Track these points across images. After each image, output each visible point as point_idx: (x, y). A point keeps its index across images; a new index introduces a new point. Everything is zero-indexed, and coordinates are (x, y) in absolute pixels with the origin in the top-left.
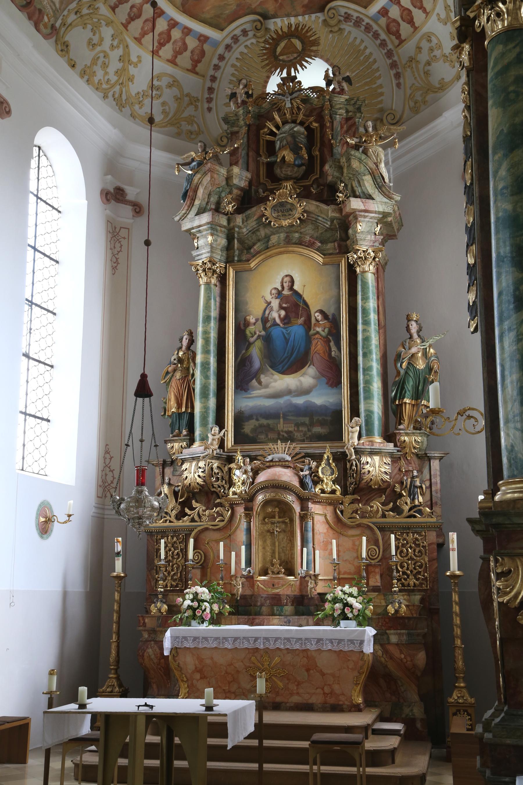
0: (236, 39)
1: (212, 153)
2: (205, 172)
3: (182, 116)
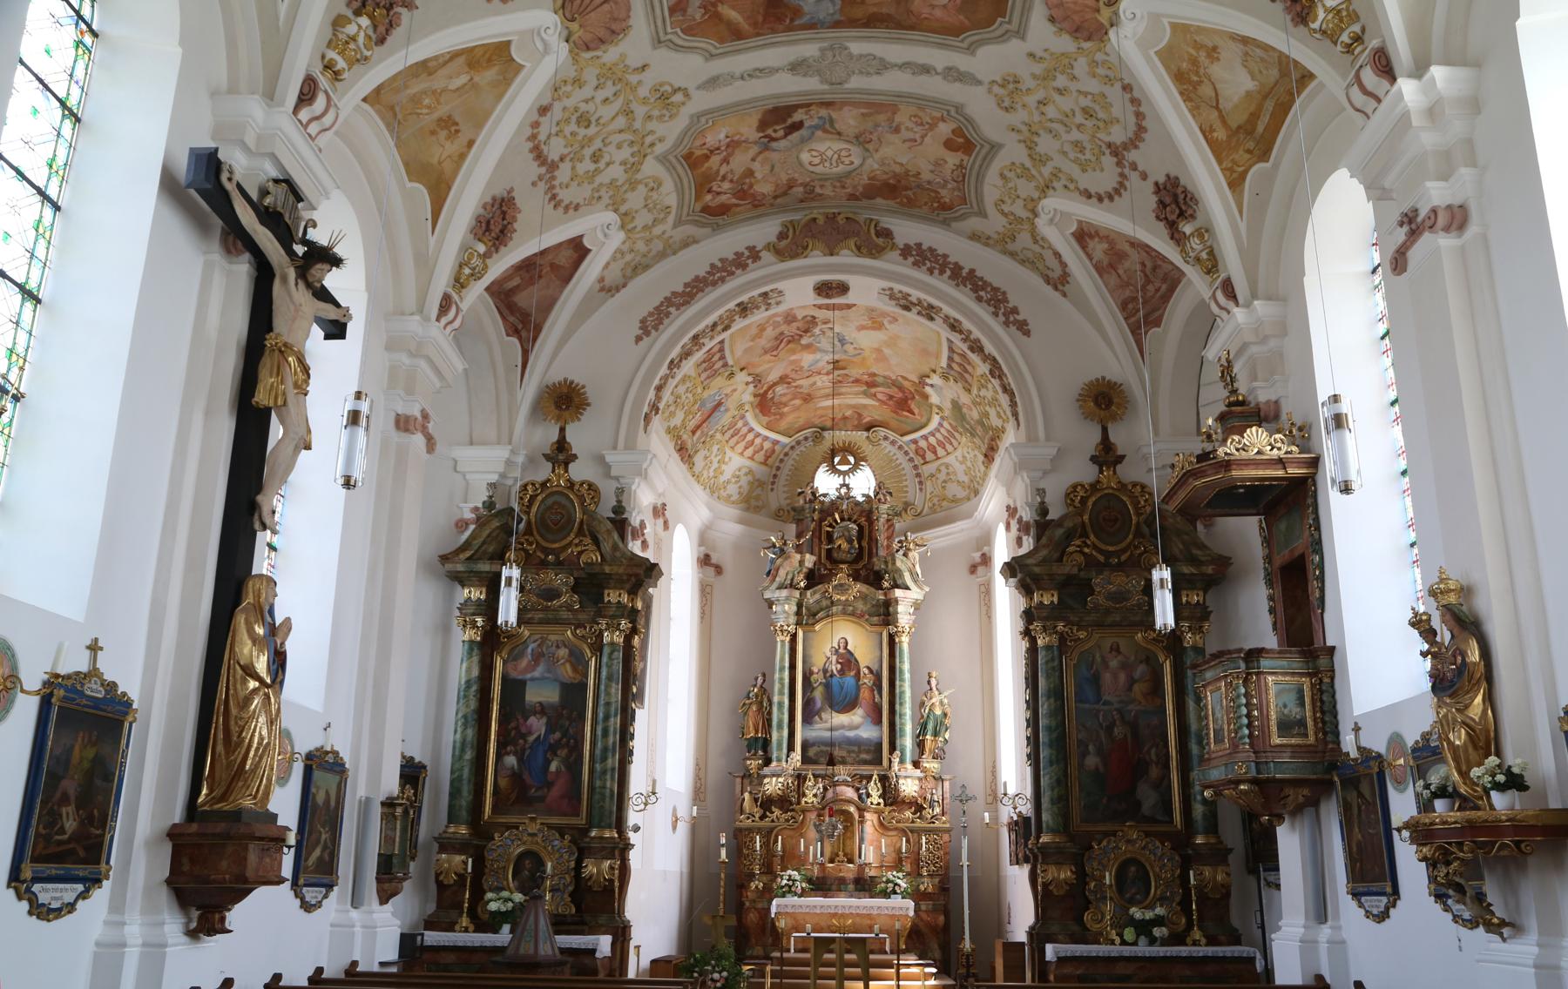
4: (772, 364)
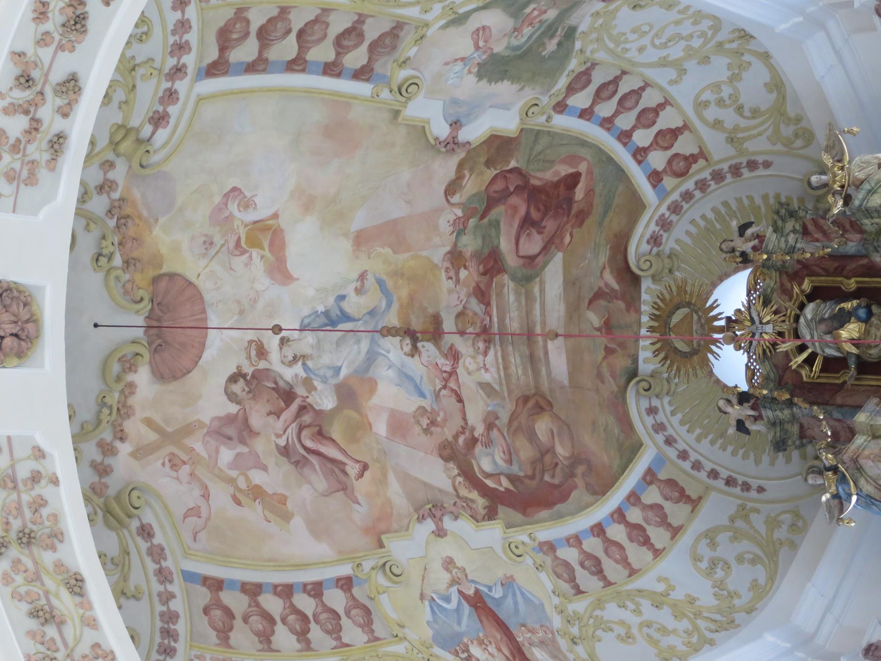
0: (659, 427)
1: (826, 454)
2: (858, 469)
3: (764, 535)
4: (392, 478)
